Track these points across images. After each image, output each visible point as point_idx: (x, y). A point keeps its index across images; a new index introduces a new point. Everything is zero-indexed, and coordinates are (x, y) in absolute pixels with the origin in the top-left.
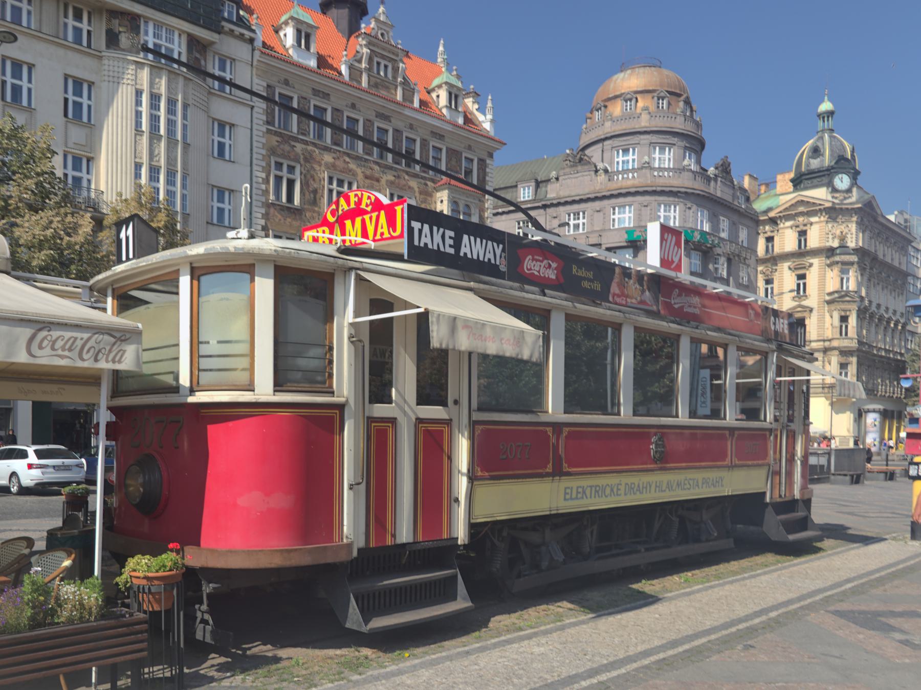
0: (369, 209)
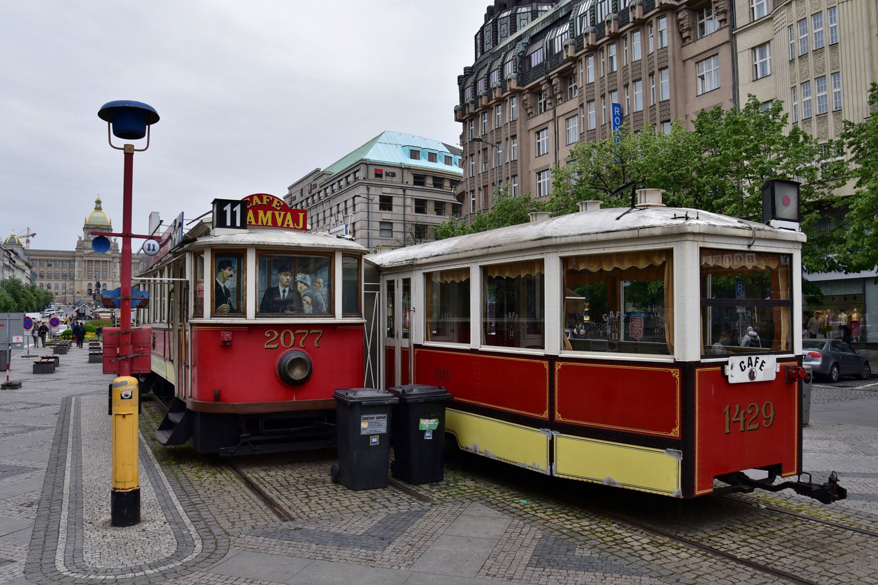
0: (279, 208)
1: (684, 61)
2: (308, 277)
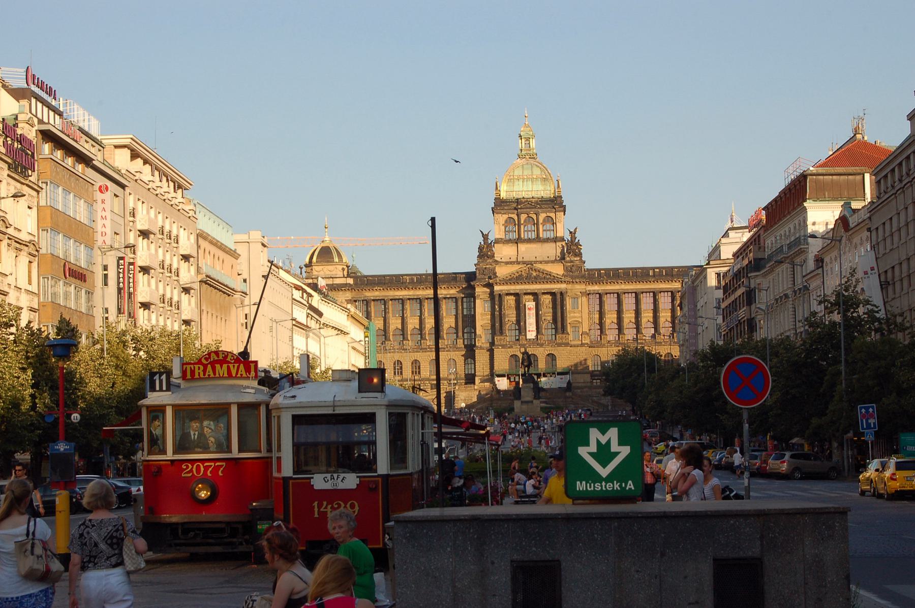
0: (233, 361)
2: (212, 423)
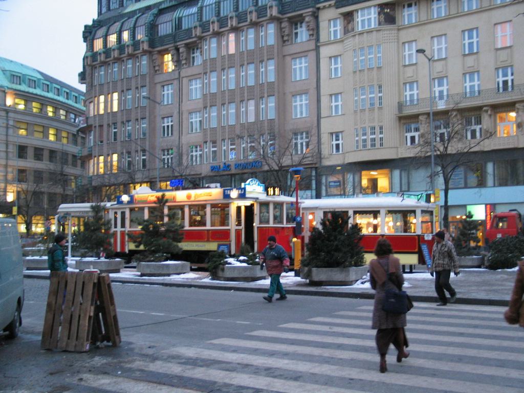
1: (284, 56)
